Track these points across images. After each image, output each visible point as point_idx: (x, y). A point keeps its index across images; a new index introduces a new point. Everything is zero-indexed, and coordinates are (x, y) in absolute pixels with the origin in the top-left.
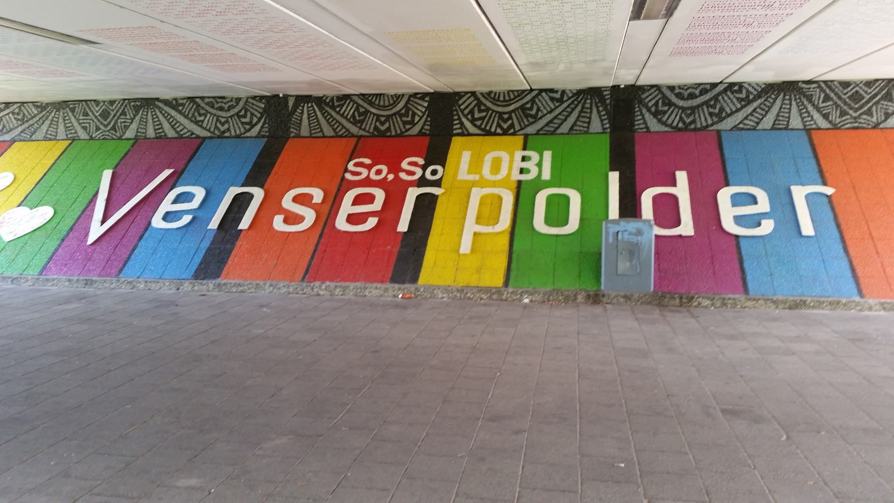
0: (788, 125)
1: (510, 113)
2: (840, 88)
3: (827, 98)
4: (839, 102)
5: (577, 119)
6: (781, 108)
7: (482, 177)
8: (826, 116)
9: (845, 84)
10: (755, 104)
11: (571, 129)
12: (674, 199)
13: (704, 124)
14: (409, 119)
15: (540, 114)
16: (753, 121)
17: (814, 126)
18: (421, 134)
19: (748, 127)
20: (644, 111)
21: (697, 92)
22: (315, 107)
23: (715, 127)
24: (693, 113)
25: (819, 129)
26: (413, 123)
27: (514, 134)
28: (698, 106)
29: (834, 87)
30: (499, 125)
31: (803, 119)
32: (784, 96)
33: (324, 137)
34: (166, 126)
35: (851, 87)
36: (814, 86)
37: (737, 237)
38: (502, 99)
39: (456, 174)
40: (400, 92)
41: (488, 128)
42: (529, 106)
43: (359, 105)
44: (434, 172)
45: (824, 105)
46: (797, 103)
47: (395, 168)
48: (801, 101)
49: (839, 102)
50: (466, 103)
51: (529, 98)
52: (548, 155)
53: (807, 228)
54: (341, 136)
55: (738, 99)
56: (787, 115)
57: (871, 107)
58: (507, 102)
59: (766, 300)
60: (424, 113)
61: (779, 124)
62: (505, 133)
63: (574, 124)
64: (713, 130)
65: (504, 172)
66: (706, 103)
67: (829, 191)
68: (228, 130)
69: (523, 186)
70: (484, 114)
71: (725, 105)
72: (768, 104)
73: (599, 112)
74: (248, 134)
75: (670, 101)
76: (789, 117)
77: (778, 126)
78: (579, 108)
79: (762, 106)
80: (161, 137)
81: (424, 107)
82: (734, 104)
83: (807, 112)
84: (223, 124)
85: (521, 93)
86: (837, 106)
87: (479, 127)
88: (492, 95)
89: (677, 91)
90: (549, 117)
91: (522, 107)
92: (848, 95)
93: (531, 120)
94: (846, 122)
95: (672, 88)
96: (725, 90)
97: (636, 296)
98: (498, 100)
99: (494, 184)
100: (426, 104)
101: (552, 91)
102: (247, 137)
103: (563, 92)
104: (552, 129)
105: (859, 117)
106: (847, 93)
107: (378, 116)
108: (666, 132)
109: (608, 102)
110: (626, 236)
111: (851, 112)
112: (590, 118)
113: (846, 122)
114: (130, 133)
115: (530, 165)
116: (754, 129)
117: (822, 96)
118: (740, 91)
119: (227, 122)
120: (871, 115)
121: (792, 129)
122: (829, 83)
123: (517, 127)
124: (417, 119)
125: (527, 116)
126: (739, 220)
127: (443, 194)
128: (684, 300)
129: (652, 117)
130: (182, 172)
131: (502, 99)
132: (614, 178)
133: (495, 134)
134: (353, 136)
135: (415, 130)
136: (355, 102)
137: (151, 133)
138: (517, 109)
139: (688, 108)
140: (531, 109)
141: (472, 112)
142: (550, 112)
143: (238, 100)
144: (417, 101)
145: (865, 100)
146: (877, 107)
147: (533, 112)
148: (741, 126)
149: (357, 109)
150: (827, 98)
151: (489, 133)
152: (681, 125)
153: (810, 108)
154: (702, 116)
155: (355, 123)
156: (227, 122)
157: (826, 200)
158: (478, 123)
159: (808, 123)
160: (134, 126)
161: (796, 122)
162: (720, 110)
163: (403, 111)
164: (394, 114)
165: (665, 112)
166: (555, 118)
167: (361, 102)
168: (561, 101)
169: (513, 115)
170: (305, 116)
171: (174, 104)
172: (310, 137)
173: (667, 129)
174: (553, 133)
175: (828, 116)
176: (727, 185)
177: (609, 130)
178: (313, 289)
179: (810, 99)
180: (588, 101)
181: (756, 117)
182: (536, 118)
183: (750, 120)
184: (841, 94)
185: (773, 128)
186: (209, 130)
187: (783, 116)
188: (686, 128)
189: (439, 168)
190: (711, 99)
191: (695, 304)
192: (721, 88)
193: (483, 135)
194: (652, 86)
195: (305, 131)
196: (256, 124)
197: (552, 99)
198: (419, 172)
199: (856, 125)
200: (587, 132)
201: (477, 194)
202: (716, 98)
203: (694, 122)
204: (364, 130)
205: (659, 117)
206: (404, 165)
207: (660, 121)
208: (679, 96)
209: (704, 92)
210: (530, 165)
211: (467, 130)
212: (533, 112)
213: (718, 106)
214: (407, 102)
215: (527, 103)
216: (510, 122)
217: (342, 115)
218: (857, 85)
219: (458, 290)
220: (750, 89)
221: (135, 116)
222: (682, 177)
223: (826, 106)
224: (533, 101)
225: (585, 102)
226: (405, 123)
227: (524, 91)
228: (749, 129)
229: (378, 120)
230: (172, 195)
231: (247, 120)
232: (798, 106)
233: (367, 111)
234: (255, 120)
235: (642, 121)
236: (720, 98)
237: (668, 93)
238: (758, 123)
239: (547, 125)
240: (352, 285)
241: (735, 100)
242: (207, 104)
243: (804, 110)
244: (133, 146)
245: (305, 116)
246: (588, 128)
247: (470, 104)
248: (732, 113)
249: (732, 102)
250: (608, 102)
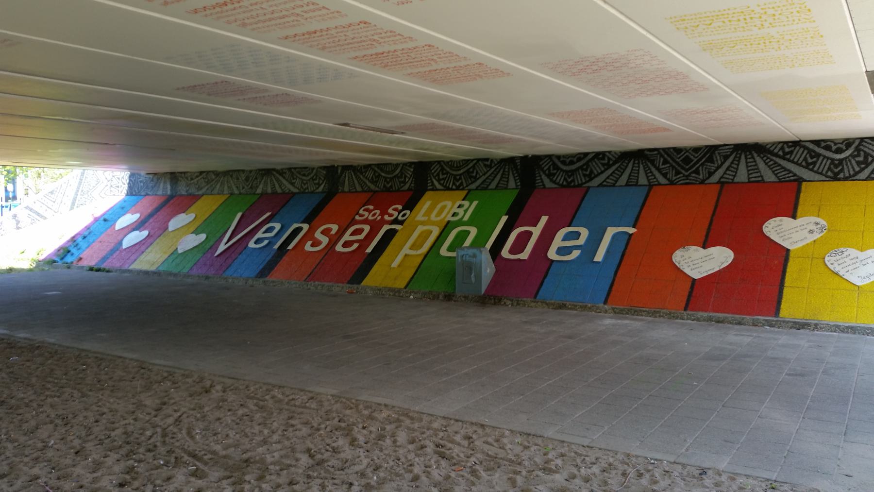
0: (637, 182)
1: (460, 175)
2: (675, 154)
3: (665, 162)
4: (674, 164)
5: (500, 180)
6: (632, 169)
7: (429, 219)
8: (665, 175)
9: (678, 150)
10: (614, 168)
11: (497, 186)
12: (529, 234)
13: (580, 182)
14: (403, 179)
15: (478, 176)
16: (613, 180)
17: (656, 183)
18: (409, 189)
19: (609, 184)
20: (542, 173)
21: (575, 160)
22: (352, 173)
23: (587, 185)
24: (573, 175)
25: (660, 184)
26: (405, 183)
27: (463, 189)
28: (577, 169)
29: (670, 153)
30: (454, 184)
31: (648, 177)
32: (634, 161)
33: (356, 192)
34: (277, 186)
35: (683, 153)
36: (656, 152)
37: (552, 261)
38: (455, 165)
39: (416, 216)
40: (399, 162)
41: (448, 185)
42: (471, 170)
43: (375, 171)
44: (404, 215)
45: (663, 166)
46: (644, 166)
47: (384, 212)
48: (647, 165)
49: (674, 164)
50: (435, 169)
51: (471, 165)
52: (475, 203)
53: (599, 257)
54: (366, 191)
55: (601, 164)
56: (636, 175)
57: (698, 167)
58: (458, 168)
59: (541, 302)
60: (411, 176)
61: (632, 182)
62: (458, 189)
63: (499, 183)
64: (585, 187)
65: (443, 215)
66: (581, 167)
67: (632, 230)
68: (307, 188)
69: (449, 225)
70: (445, 176)
71: (593, 169)
72: (622, 167)
73: (513, 174)
74: (317, 191)
75: (558, 166)
76: (638, 177)
77: (631, 183)
78: (502, 171)
79: (619, 169)
80: (275, 193)
81: (410, 171)
82: (599, 168)
83: (651, 172)
84: (305, 184)
85: (467, 162)
86: (673, 167)
87: (442, 185)
88: (450, 163)
89: (562, 159)
90: (484, 178)
91: (468, 171)
92: (681, 159)
93: (473, 180)
94: (680, 179)
95: (558, 157)
96: (593, 158)
97: (470, 297)
98: (453, 166)
99: (434, 223)
100: (412, 170)
101: (487, 160)
102: (317, 193)
103: (492, 161)
104: (486, 186)
105: (689, 175)
106: (680, 157)
107: (386, 178)
108: (556, 188)
109: (519, 167)
110: (468, 258)
111: (683, 172)
112: (508, 178)
113: (680, 179)
114: (259, 191)
116: (614, 185)
117: (662, 160)
118: (603, 159)
119: (307, 183)
120: (698, 173)
121: (640, 185)
122: (667, 150)
123: (465, 185)
124: (407, 180)
125: (471, 177)
126: (561, 251)
127: (402, 229)
128: (496, 301)
129: (546, 178)
130: (276, 214)
131: (455, 165)
132: (504, 218)
133: (452, 189)
134: (372, 191)
135: (406, 187)
136: (373, 169)
138: (464, 172)
139: (570, 171)
140: (473, 172)
141: (438, 175)
142: (484, 175)
143: (313, 169)
144: (407, 167)
145: (693, 163)
146: (702, 167)
147: (474, 174)
148: (605, 183)
149: (374, 174)
150: (665, 162)
151: (448, 189)
152: (565, 183)
153: (653, 169)
154: (579, 177)
155: (372, 181)
156: (307, 183)
157: (627, 237)
158: (442, 182)
159: (651, 181)
160: (261, 186)
161: (643, 180)
162: (590, 171)
163: (399, 175)
164: (395, 177)
165: (554, 174)
166: (487, 178)
167: (376, 169)
168: (490, 167)
169: (462, 177)
170: (347, 178)
171: (281, 172)
172: (350, 192)
173: (556, 186)
174: (486, 189)
175: (667, 176)
176: (569, 226)
177: (519, 187)
178: (307, 286)
179: (652, 162)
180: (507, 167)
181: (615, 177)
182: (476, 179)
183: (611, 179)
184: (675, 158)
185: (627, 185)
186: (298, 188)
187: (633, 176)
188: (568, 185)
189: (408, 212)
190: (584, 165)
191: (503, 303)
192: (590, 156)
193: (445, 190)
194: (546, 156)
195: (346, 189)
196: (322, 184)
197: (485, 166)
198: (396, 214)
199: (688, 181)
200: (506, 188)
201: (420, 229)
202: (587, 164)
203: (573, 181)
204: (378, 187)
205: (552, 177)
206: (390, 211)
207: (551, 180)
208: (564, 163)
209: (579, 159)
210: (461, 211)
211: (436, 187)
212: (474, 174)
213: (589, 170)
214: (401, 170)
215: (470, 168)
216: (460, 181)
217: (366, 178)
218: (687, 151)
219: (378, 290)
220: (610, 156)
221: (262, 180)
222: (544, 219)
223: (664, 168)
224: (474, 167)
225: (505, 168)
226: (401, 182)
227: (468, 160)
228: (610, 186)
229: (385, 180)
231: (317, 181)
232: (644, 168)
233: (380, 175)
234: (321, 182)
235: (540, 181)
236: (590, 163)
237: (556, 161)
238: (616, 182)
239: (482, 183)
240: (326, 284)
241: (600, 165)
242: (297, 172)
243: (649, 171)
244: (259, 198)
245: (347, 178)
246: (507, 185)
247: (437, 169)
248: (599, 174)
249: (598, 166)
250: (519, 167)
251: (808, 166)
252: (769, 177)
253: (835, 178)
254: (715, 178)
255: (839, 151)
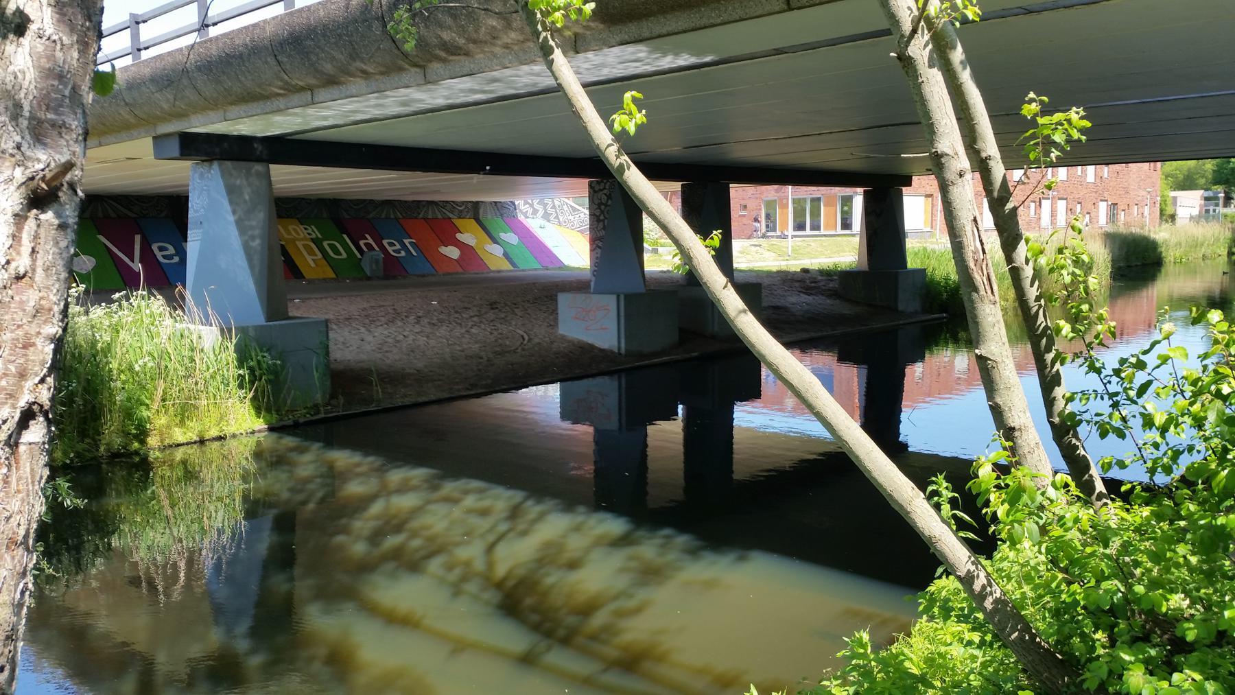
34: (110, 211)
52: (313, 227)
53: (415, 254)
62: (288, 217)
95: (351, 201)
115: (310, 231)
132: (345, 236)
137: (100, 215)
201: (299, 244)
222: (367, 236)
230: (155, 247)
251: (452, 212)
252: (440, 216)
253: (460, 218)
254: (421, 216)
255: (460, 206)
